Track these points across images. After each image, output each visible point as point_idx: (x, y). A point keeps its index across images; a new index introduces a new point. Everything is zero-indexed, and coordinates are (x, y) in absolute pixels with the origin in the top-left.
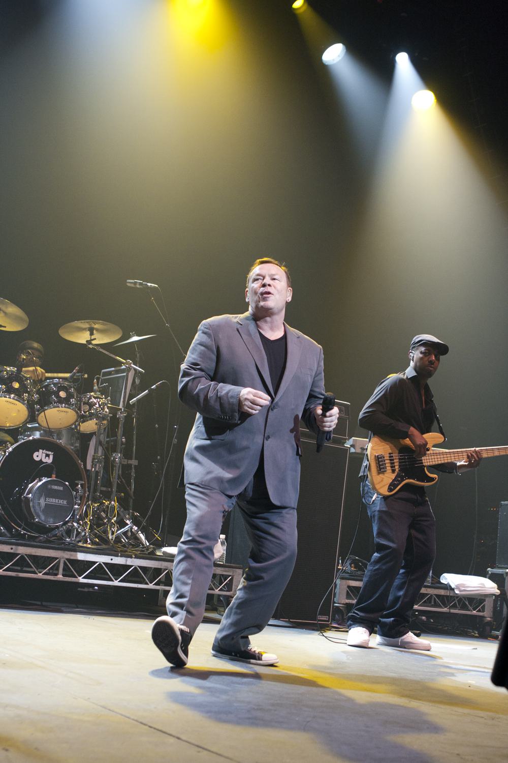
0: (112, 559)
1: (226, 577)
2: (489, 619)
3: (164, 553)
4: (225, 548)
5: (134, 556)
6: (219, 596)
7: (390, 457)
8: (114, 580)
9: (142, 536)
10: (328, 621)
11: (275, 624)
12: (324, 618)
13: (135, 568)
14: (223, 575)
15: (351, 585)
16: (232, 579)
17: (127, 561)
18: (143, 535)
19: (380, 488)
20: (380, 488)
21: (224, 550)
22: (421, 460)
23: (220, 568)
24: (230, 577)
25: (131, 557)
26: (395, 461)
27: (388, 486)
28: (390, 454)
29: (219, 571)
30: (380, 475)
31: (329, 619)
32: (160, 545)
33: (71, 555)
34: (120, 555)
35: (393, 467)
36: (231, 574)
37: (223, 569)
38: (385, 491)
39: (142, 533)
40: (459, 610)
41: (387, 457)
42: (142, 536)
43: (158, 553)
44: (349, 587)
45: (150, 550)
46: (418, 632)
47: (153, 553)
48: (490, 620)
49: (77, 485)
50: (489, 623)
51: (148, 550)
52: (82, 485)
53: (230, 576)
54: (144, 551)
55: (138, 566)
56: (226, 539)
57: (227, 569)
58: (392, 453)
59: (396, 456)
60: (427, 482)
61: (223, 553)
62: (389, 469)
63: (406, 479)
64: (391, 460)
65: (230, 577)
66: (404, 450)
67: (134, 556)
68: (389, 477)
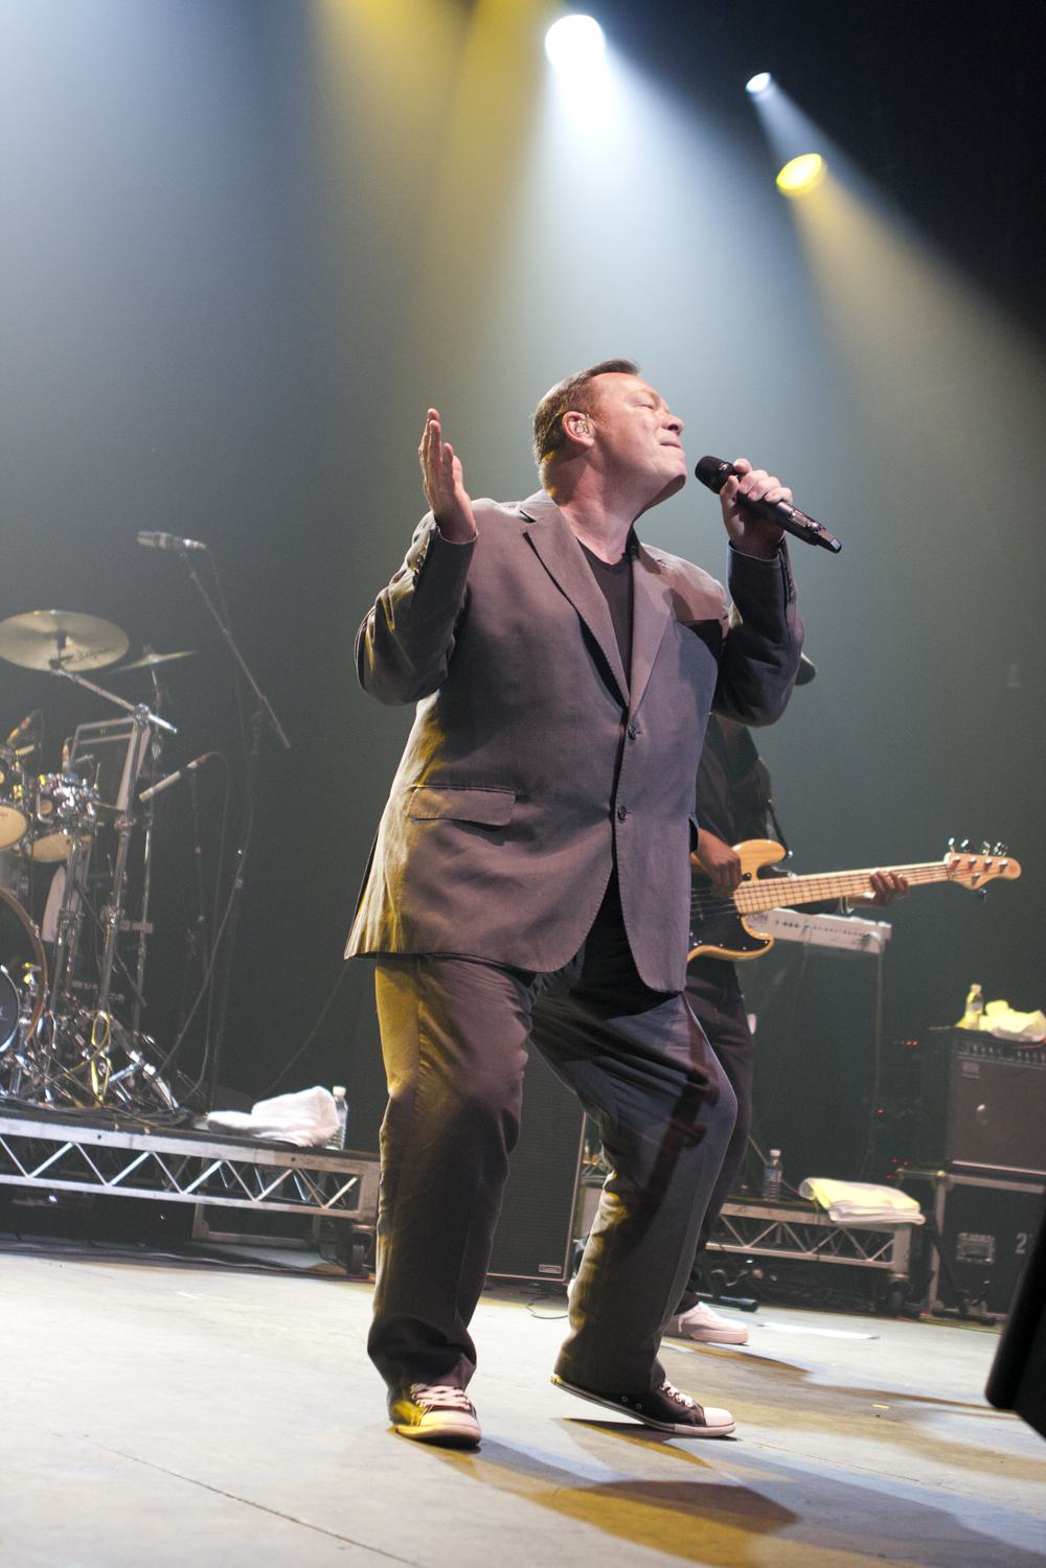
0: (100, 1137)
1: (345, 1178)
2: (900, 1276)
3: (214, 1125)
4: (344, 1115)
5: (147, 1131)
6: (325, 1218)
8: (103, 1181)
9: (164, 1088)
10: (560, 1276)
12: (553, 1269)
13: (151, 1157)
14: (336, 1174)
16: (356, 1187)
17: (131, 1140)
18: (167, 1084)
21: (342, 1121)
22: (733, 901)
24: (353, 1181)
25: (142, 1133)
29: (331, 1165)
31: (563, 1271)
33: (12, 1127)
34: (117, 1126)
36: (355, 1172)
39: (164, 1081)
40: (836, 1255)
43: (203, 1126)
45: (182, 1118)
46: (752, 1301)
48: (903, 1279)
49: (26, 972)
50: (898, 1285)
51: (175, 1117)
52: (36, 975)
53: (350, 1177)
54: (167, 1120)
55: (158, 1153)
57: (348, 1161)
60: (748, 950)
61: (341, 1128)
63: (700, 945)
65: (353, 1181)
67: (147, 1131)
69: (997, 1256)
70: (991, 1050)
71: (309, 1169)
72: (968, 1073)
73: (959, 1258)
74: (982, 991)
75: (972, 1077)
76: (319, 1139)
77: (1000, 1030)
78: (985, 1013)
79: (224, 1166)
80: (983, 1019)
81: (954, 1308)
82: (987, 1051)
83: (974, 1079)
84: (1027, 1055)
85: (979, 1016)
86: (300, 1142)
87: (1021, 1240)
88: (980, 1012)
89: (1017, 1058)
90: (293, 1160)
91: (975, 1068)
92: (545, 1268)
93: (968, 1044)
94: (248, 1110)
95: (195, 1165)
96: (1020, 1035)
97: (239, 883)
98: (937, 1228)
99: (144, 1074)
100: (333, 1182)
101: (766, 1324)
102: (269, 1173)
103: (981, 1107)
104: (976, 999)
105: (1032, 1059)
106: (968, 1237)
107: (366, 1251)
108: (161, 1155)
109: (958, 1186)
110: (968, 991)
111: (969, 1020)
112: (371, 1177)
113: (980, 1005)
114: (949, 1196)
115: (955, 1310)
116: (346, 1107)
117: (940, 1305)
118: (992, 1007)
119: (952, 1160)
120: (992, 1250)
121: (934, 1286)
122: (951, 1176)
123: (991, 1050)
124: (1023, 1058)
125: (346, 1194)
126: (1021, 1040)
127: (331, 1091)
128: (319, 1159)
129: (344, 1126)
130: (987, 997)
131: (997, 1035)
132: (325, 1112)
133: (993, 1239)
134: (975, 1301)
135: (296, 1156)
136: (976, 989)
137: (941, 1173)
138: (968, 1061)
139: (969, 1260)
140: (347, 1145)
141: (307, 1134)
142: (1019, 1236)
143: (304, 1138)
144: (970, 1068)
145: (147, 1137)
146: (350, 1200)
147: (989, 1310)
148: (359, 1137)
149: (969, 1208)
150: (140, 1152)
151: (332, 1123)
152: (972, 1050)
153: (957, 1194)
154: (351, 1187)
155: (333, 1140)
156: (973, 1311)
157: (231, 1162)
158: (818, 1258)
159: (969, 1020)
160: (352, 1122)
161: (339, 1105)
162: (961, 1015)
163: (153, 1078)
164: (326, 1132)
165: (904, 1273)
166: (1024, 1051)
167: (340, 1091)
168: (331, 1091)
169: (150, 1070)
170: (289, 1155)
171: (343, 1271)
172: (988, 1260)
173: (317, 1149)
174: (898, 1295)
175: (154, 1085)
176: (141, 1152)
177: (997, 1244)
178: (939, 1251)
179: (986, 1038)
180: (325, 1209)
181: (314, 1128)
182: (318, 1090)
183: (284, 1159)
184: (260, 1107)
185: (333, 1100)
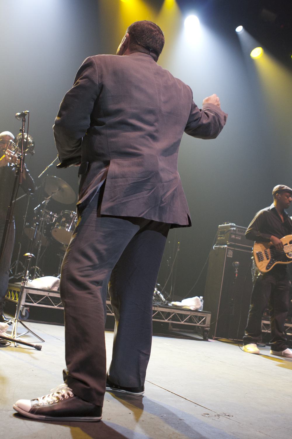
1: (203, 317)
3: (173, 305)
4: (202, 303)
6: (198, 327)
7: (265, 252)
9: (162, 296)
13: (159, 312)
14: (201, 317)
16: (205, 319)
19: (261, 269)
20: (261, 269)
23: (200, 313)
25: (157, 306)
26: (268, 253)
27: (266, 267)
28: (265, 250)
29: (199, 314)
30: (261, 262)
32: (170, 300)
35: (267, 257)
36: (205, 316)
37: (201, 313)
38: (264, 270)
39: (162, 295)
41: (263, 252)
42: (162, 296)
43: (170, 305)
45: (166, 303)
47: (167, 305)
51: (164, 303)
53: (204, 317)
54: (162, 303)
56: (203, 299)
58: (266, 250)
59: (268, 251)
61: (202, 306)
62: (265, 258)
64: (265, 253)
66: (272, 248)
68: (266, 262)
71: (194, 316)
76: (196, 308)
79: (175, 314)
86: (192, 309)
90: (191, 313)
94: (181, 302)
95: (169, 314)
97: (178, 250)
99: (157, 293)
100: (200, 318)
102: (186, 316)
107: (207, 334)
108: (161, 311)
112: (208, 317)
116: (203, 301)
125: (203, 321)
127: (199, 297)
128: (197, 313)
129: (202, 305)
132: (198, 302)
135: (191, 312)
140: (203, 310)
141: (194, 307)
143: (193, 308)
145: (158, 308)
146: (204, 322)
148: (206, 307)
150: (157, 311)
151: (199, 305)
154: (204, 319)
155: (200, 308)
157: (177, 313)
160: (204, 304)
161: (201, 301)
163: (160, 294)
164: (198, 307)
167: (201, 297)
168: (199, 297)
169: (159, 292)
170: (190, 312)
171: (202, 338)
173: (196, 311)
175: (160, 296)
176: (157, 311)
180: (198, 324)
181: (195, 306)
182: (197, 297)
183: (188, 313)
184: (183, 301)
185: (200, 299)
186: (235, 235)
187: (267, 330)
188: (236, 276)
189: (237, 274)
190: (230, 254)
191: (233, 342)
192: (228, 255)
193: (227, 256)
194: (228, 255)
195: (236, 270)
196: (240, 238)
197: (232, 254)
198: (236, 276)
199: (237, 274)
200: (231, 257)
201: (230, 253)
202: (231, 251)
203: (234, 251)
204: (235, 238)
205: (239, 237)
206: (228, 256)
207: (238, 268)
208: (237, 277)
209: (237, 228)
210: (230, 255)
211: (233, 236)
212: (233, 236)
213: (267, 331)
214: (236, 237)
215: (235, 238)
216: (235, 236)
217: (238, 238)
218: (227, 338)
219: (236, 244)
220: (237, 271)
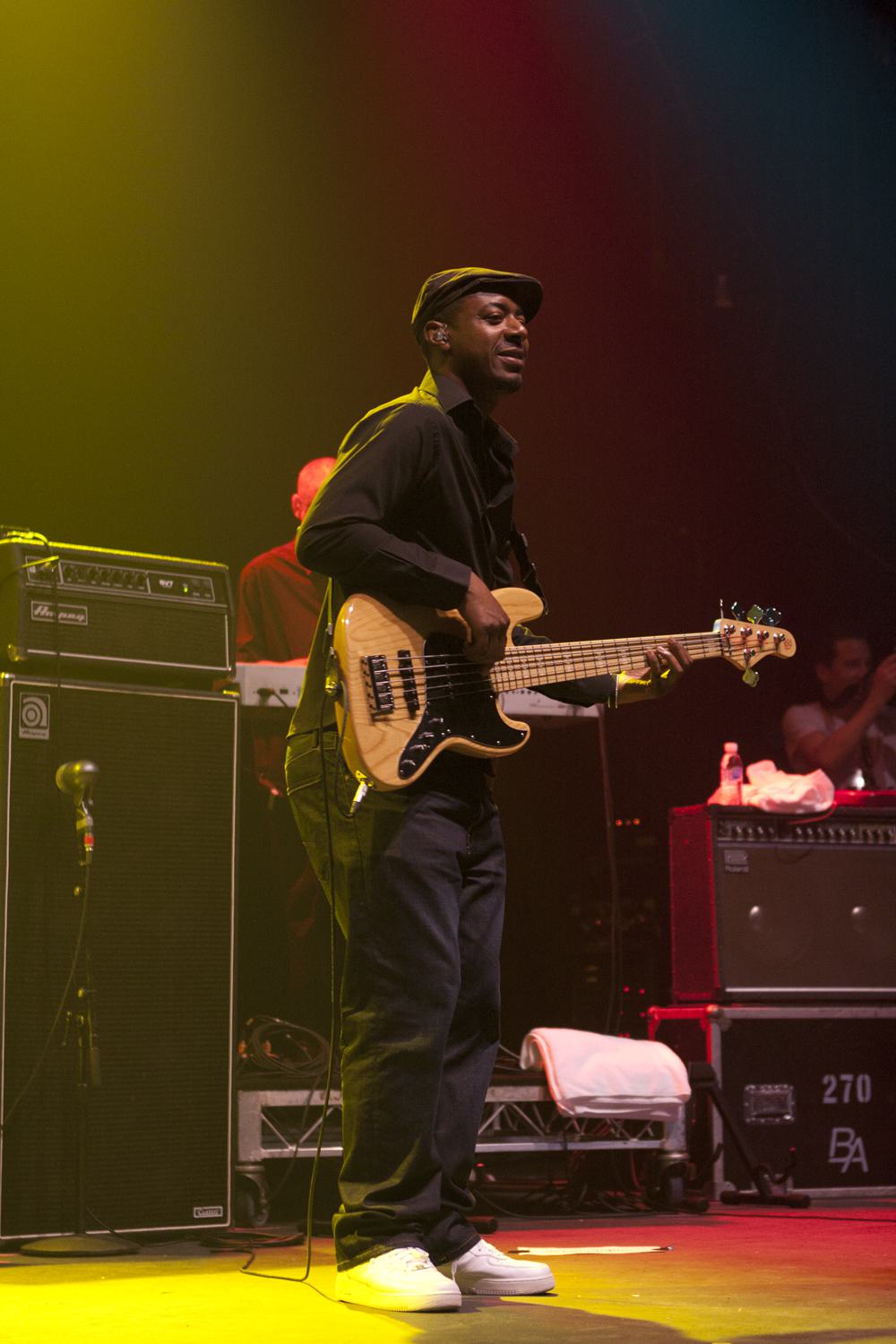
10: (223, 1220)
11: (78, 1248)
12: (212, 1212)
15: (272, 1104)
40: (582, 1140)
44: (269, 1111)
46: (489, 1219)
48: (682, 1160)
50: (678, 1168)
69: (798, 1111)
70: (761, 830)
72: (732, 866)
73: (748, 1120)
74: (739, 751)
75: (738, 870)
77: (770, 802)
78: (746, 781)
80: (746, 789)
81: (749, 1188)
82: (755, 831)
83: (741, 873)
84: (810, 831)
85: (739, 784)
87: (829, 1083)
88: (741, 779)
89: (796, 836)
91: (742, 857)
92: (200, 1212)
93: (729, 826)
96: (798, 805)
98: (716, 1085)
101: (520, 1249)
103: (755, 910)
104: (731, 765)
105: (816, 835)
106: (758, 1089)
109: (736, 1022)
110: (723, 752)
111: (726, 792)
113: (737, 770)
114: (725, 1036)
115: (753, 1191)
117: (730, 1187)
118: (754, 771)
119: (724, 988)
120: (791, 1103)
121: (719, 1165)
122: (726, 1009)
123: (761, 830)
124: (805, 835)
126: (800, 811)
130: (747, 758)
131: (766, 808)
133: (792, 1088)
134: (778, 1176)
136: (731, 747)
137: (712, 1008)
138: (728, 848)
139: (763, 1120)
142: (826, 1080)
144: (735, 858)
147: (796, 1186)
149: (757, 1050)
152: (735, 834)
153: (737, 1033)
156: (776, 1191)
158: (565, 1142)
159: (726, 792)
162: (715, 784)
165: (680, 1152)
166: (804, 828)
172: (788, 1117)
174: (676, 1183)
177: (797, 1096)
178: (721, 1112)
179: (752, 814)
186: (54, 598)
187: (294, 1141)
188: (89, 848)
189: (89, 835)
190: (36, 722)
191: (119, 1247)
192: (25, 726)
193: (15, 732)
194: (25, 726)
195: (86, 811)
196: (81, 618)
197: (44, 723)
198: (89, 848)
199: (89, 835)
200: (45, 735)
201: (31, 715)
202: (40, 702)
203: (58, 701)
204: (55, 618)
205: (77, 612)
206: (21, 735)
207: (91, 802)
208: (93, 853)
209: (63, 554)
210: (38, 727)
211: (42, 611)
212: (42, 611)
213: (293, 1148)
214: (62, 615)
215: (55, 618)
216: (51, 609)
217: (71, 616)
218: (79, 1231)
219: (62, 654)
220: (86, 821)
